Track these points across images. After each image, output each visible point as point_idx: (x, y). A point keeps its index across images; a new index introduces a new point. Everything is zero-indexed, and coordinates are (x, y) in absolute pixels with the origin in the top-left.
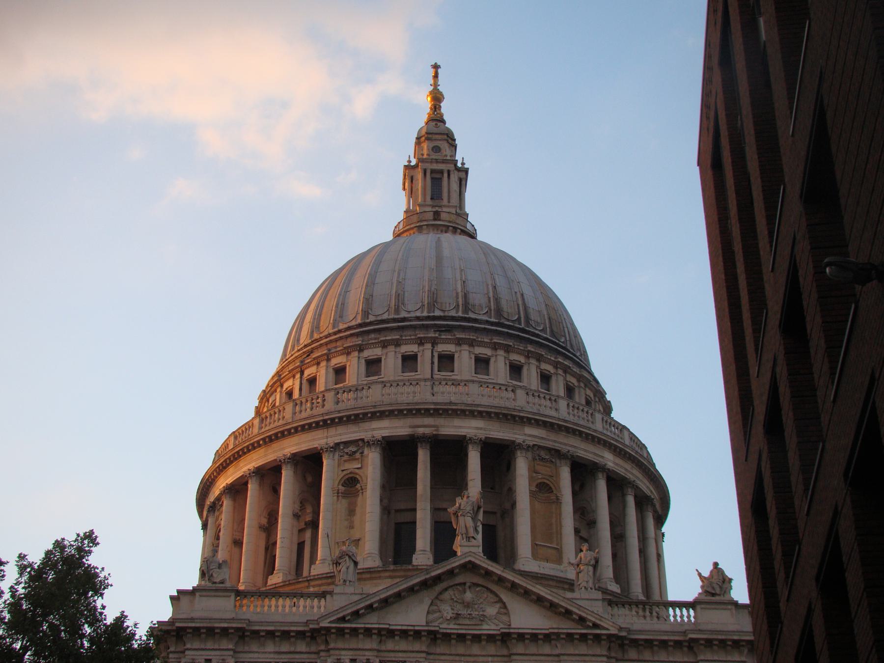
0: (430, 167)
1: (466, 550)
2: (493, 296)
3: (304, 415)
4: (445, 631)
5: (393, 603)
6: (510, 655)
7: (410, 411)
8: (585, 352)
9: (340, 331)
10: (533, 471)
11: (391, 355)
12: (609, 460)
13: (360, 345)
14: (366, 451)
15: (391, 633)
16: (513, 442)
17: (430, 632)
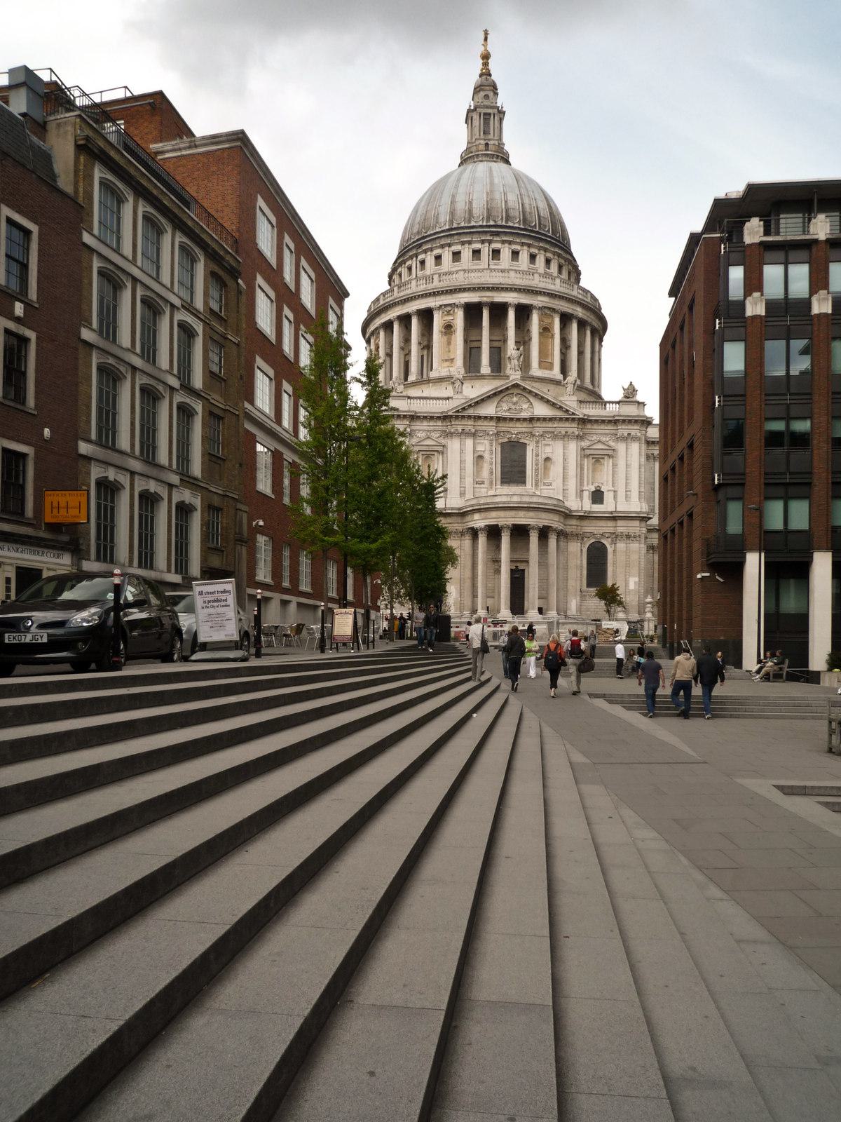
3: (422, 287)
7: (479, 288)
8: (569, 239)
11: (466, 250)
12: (579, 312)
14: (456, 310)
15: (480, 418)
16: (532, 305)
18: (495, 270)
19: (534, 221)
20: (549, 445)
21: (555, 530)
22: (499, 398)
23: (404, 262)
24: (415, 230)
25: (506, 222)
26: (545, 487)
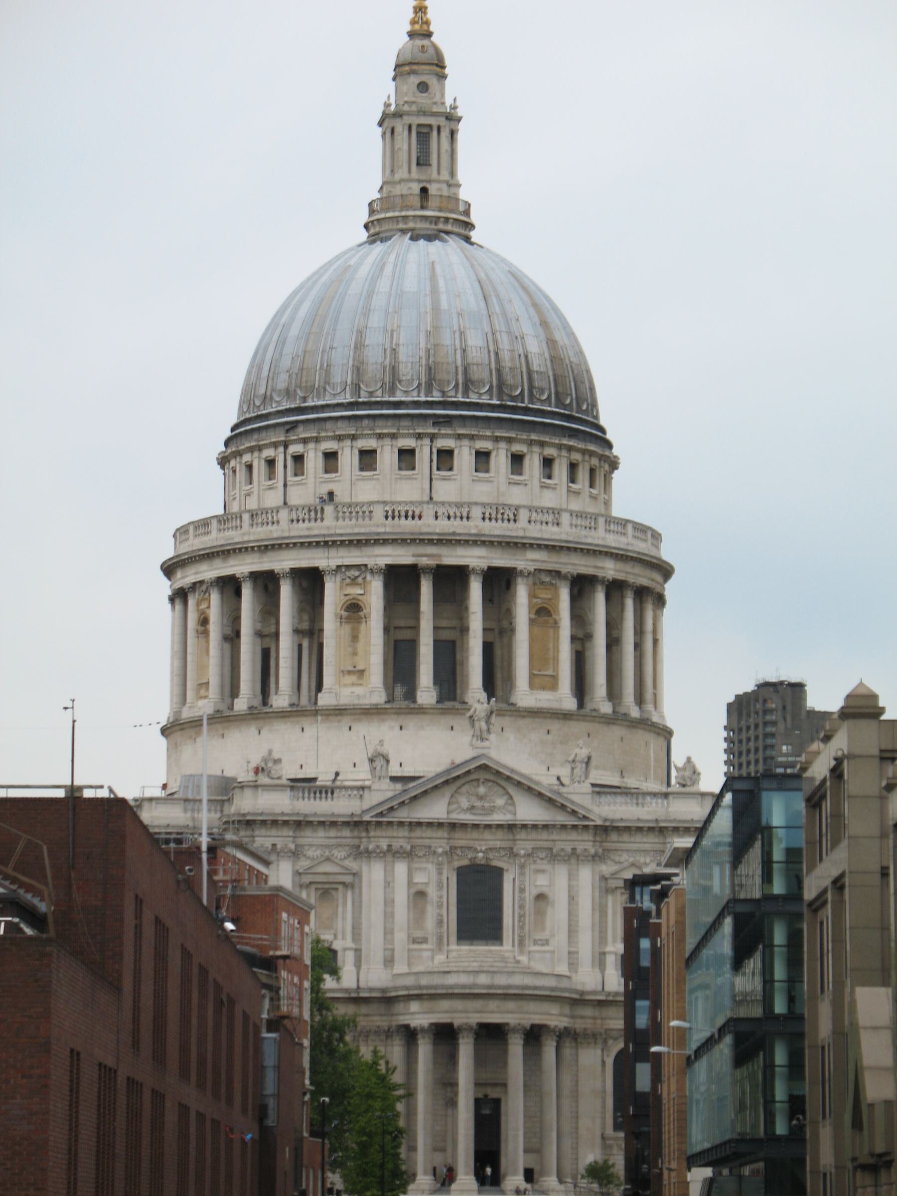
0: (416, 121)
1: (480, 751)
2: (496, 369)
4: (463, 822)
5: (420, 797)
6: (516, 840)
7: (413, 541)
8: (592, 389)
9: (328, 406)
10: (532, 596)
11: (387, 449)
12: (610, 570)
13: (353, 435)
14: (369, 577)
15: (419, 824)
16: (515, 569)
17: (450, 824)
18: (443, 503)
19: (517, 384)
20: (543, 871)
21: (553, 1031)
22: (453, 787)
23: (260, 448)
24: (282, 382)
25: (466, 393)
26: (537, 948)
